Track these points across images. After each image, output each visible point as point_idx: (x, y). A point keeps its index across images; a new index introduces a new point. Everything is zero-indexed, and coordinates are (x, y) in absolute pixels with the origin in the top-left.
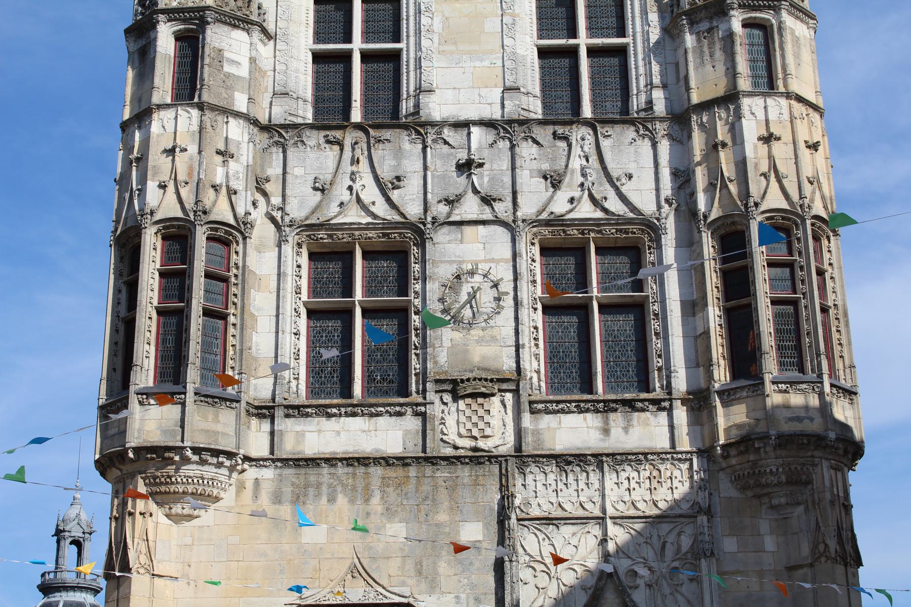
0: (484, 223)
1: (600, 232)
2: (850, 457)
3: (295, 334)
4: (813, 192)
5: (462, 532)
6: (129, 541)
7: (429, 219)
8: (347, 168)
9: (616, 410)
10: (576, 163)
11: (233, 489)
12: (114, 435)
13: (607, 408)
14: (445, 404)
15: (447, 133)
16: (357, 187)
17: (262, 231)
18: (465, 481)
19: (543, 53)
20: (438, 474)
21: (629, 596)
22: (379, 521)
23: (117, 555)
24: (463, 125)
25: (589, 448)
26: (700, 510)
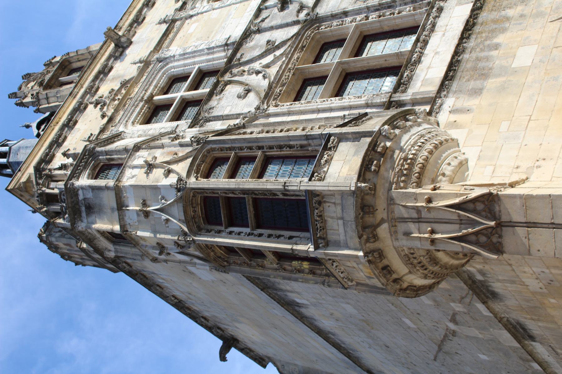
6: (457, 201)
22: (532, 6)
23: (474, 223)
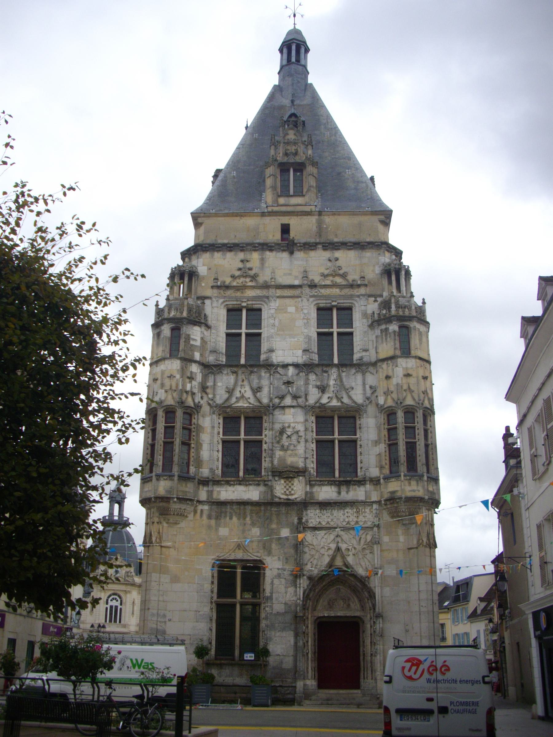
0: (293, 407)
1: (340, 411)
2: (434, 505)
3: (218, 451)
4: (424, 397)
5: (281, 532)
7: (271, 405)
8: (240, 383)
9: (343, 485)
10: (332, 383)
11: (192, 513)
12: (147, 491)
13: (339, 484)
14: (276, 481)
15: (279, 369)
16: (243, 391)
17: (206, 409)
18: (283, 512)
19: (319, 334)
20: (273, 509)
21: (346, 558)
24: (285, 366)
25: (332, 500)
26: (375, 525)
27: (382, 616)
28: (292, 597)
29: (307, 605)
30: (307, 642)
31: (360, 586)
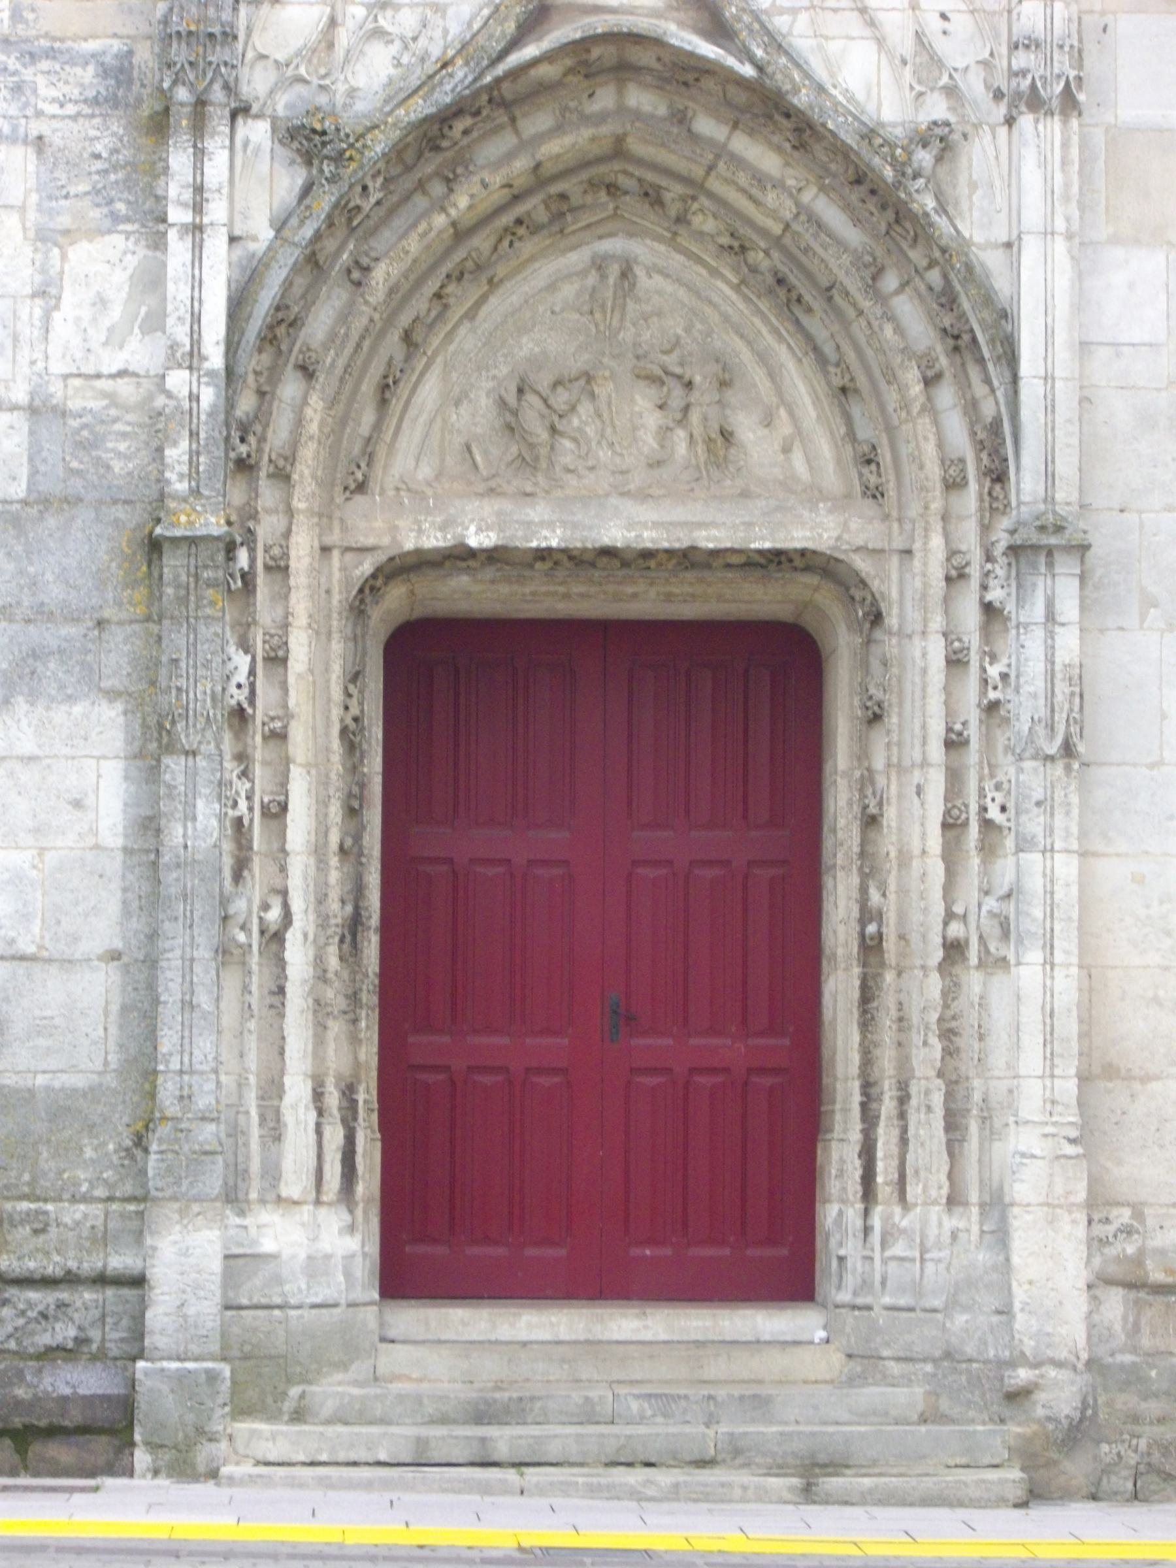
27: (1083, 549)
28: (116, 341)
29: (279, 433)
30: (277, 812)
31: (853, 236)
